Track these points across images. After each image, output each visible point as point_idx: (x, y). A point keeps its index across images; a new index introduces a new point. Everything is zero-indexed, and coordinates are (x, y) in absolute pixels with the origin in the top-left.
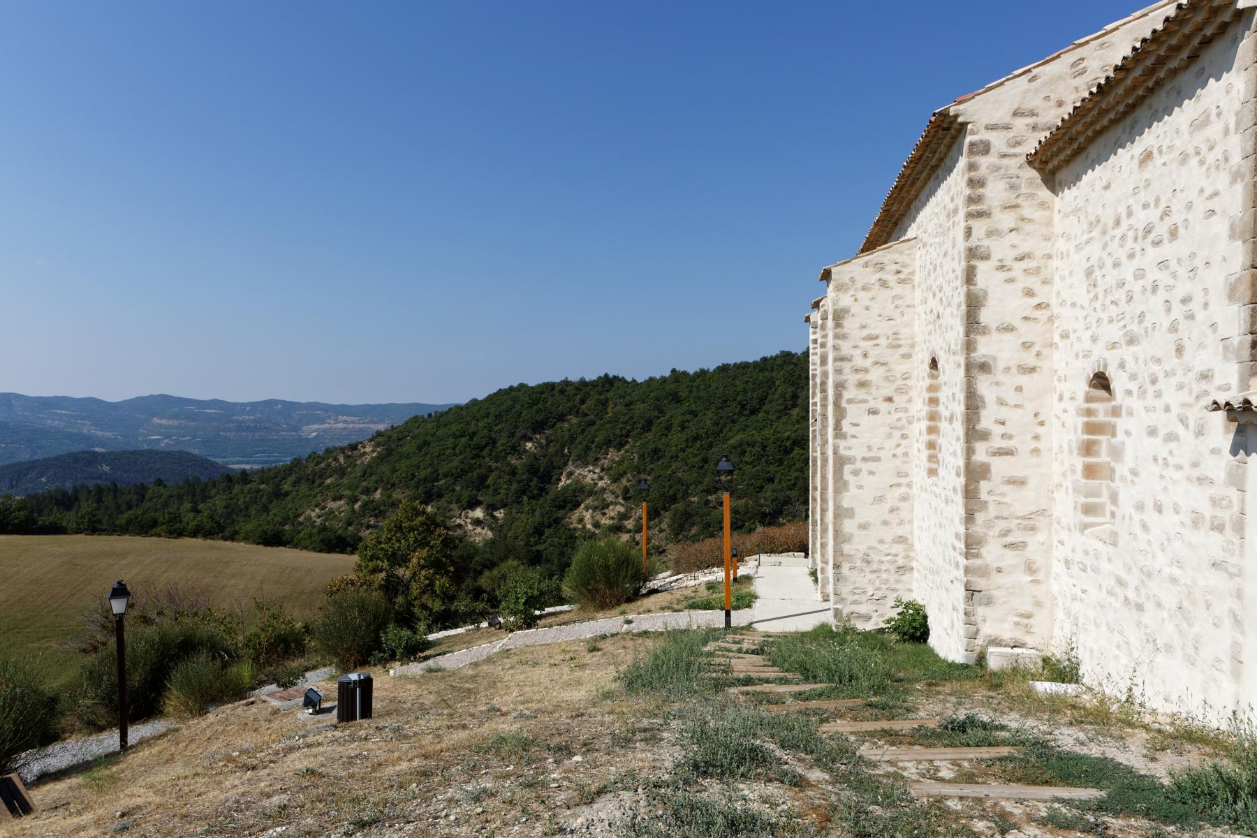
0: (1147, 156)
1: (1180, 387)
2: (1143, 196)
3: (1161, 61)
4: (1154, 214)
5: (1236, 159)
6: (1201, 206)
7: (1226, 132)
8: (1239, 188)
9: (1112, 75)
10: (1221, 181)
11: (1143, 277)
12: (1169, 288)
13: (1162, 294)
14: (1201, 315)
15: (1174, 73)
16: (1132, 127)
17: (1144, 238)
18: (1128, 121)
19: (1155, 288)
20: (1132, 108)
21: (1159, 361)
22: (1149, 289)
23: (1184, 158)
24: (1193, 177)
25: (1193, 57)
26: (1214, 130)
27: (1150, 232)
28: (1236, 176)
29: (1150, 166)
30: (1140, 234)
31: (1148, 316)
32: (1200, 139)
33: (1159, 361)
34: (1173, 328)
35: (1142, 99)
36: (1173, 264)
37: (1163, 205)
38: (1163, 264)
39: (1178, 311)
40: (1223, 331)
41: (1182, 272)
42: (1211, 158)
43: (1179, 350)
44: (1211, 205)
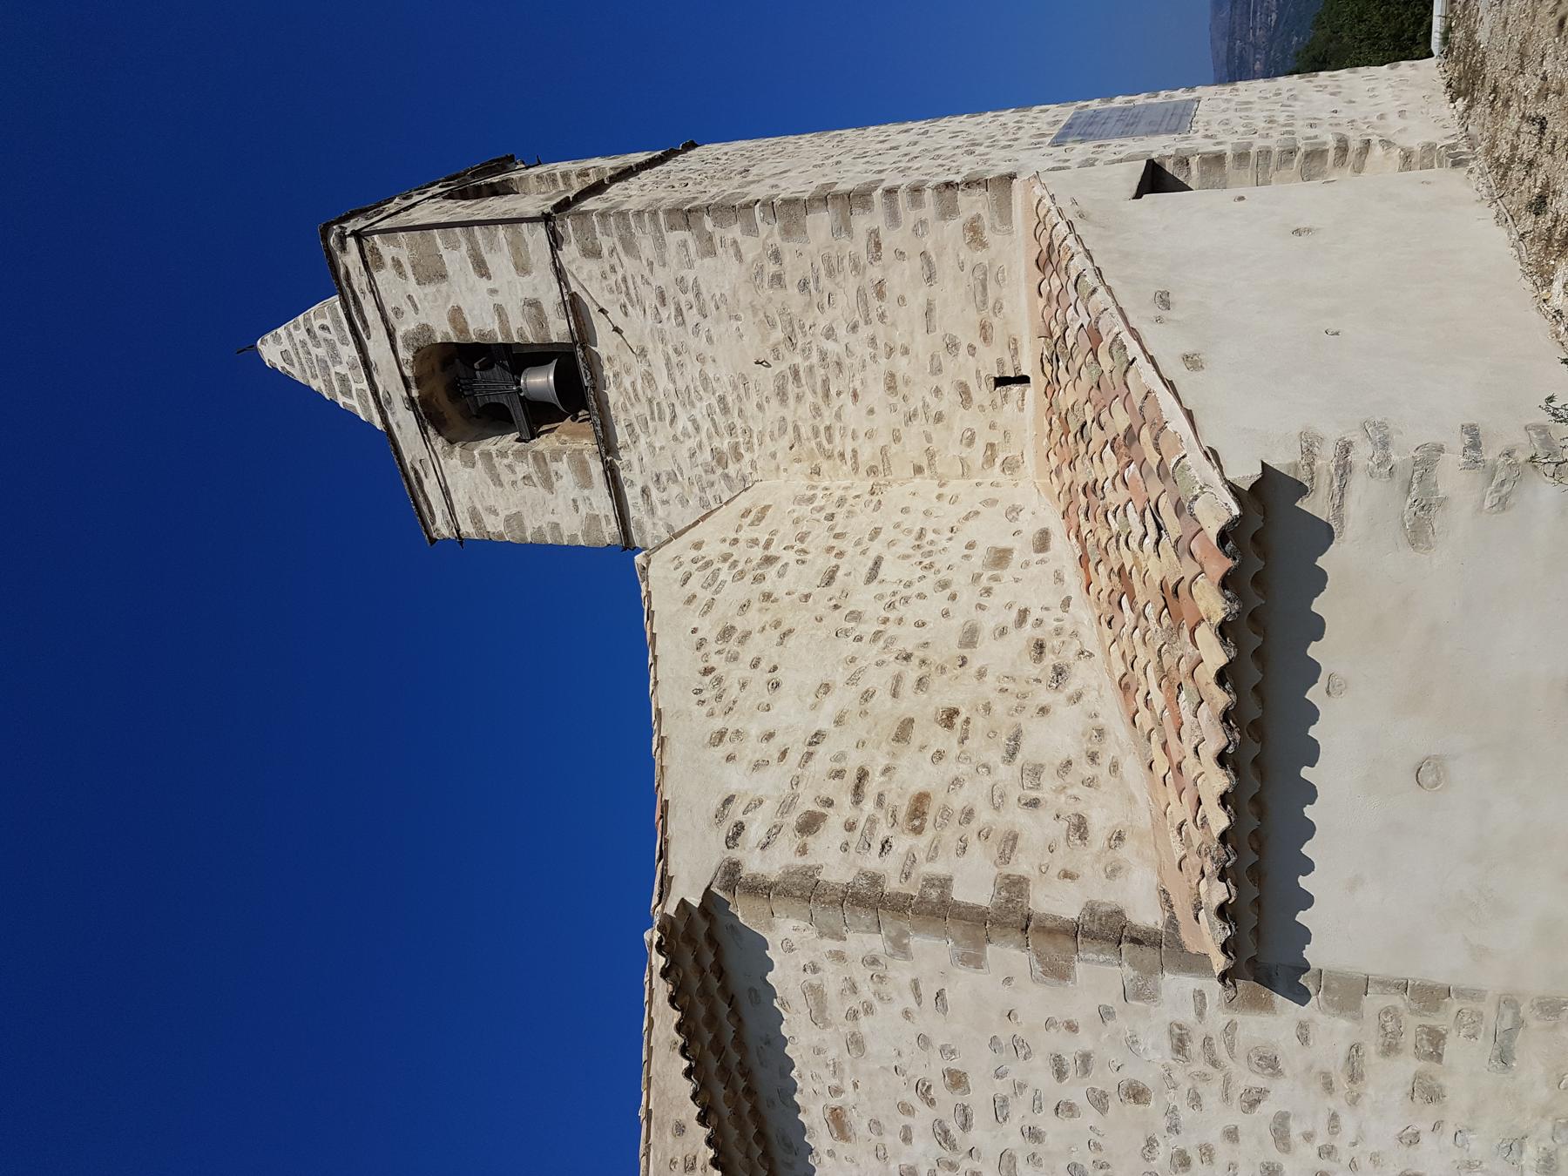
0: (837, 1120)
1: (1196, 1100)
2: (892, 1140)
3: (718, 1048)
4: (924, 1117)
5: (877, 943)
6: (928, 1020)
7: (839, 956)
8: (916, 942)
9: (708, 1131)
10: (900, 973)
11: (1012, 1158)
12: (1037, 1105)
13: (1047, 1122)
14: (1084, 1041)
15: (739, 1042)
16: (789, 1146)
17: (954, 1147)
18: (779, 1154)
19: (1034, 1135)
20: (761, 1136)
21: (1151, 1143)
22: (1033, 1147)
23: (856, 1043)
24: (886, 1030)
25: (731, 1000)
26: (831, 978)
27: (946, 1132)
28: (900, 948)
29: (851, 1116)
30: (946, 1154)
31: (1075, 1158)
32: (837, 1008)
33: (1151, 1143)
34: (1100, 1101)
35: (755, 1111)
36: (1003, 1088)
37: (912, 1098)
38: (1000, 1110)
39: (1075, 1091)
40: (1112, 999)
41: (1017, 1070)
42: (866, 991)
43: (1137, 1094)
44: (928, 995)
